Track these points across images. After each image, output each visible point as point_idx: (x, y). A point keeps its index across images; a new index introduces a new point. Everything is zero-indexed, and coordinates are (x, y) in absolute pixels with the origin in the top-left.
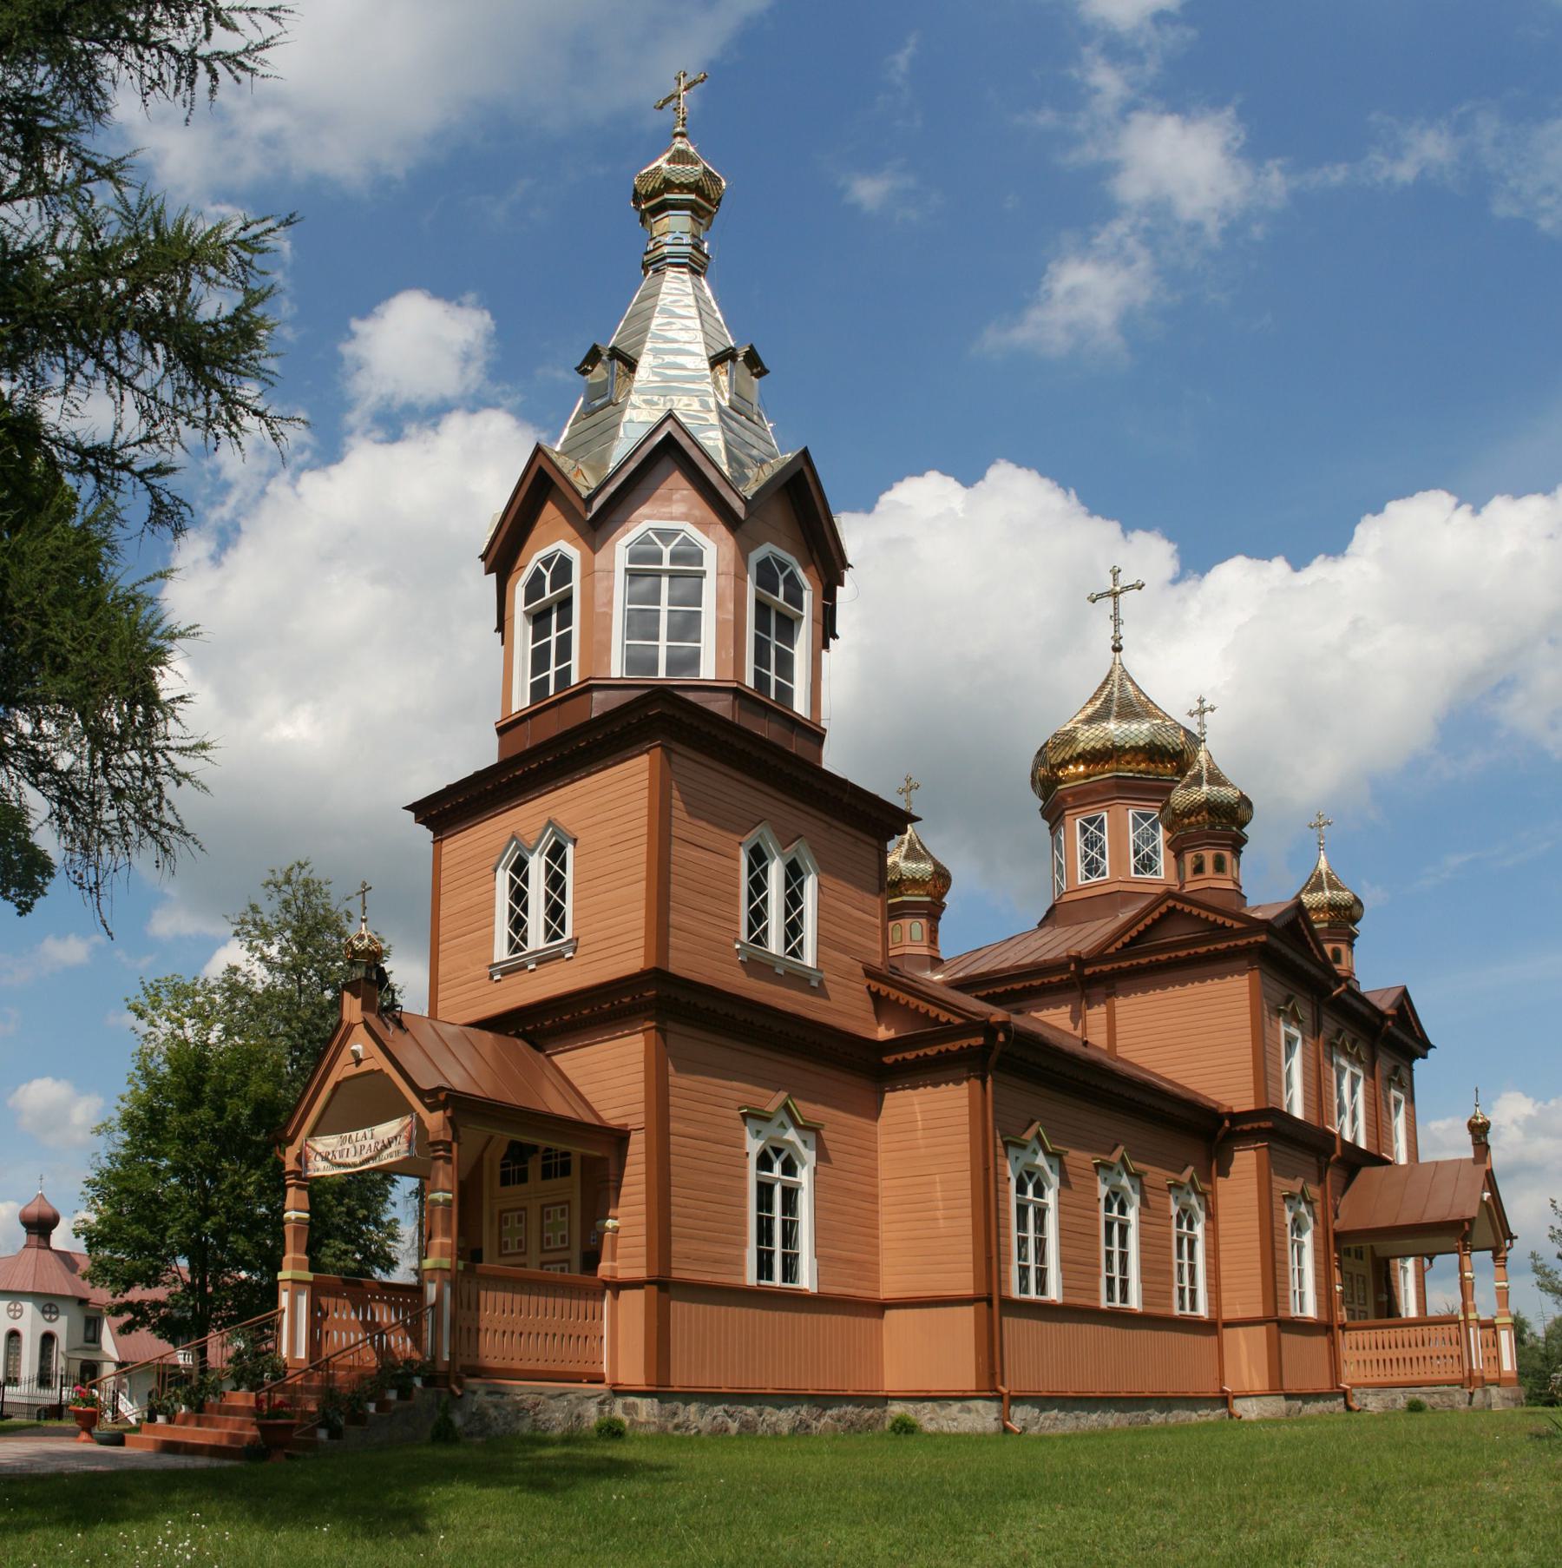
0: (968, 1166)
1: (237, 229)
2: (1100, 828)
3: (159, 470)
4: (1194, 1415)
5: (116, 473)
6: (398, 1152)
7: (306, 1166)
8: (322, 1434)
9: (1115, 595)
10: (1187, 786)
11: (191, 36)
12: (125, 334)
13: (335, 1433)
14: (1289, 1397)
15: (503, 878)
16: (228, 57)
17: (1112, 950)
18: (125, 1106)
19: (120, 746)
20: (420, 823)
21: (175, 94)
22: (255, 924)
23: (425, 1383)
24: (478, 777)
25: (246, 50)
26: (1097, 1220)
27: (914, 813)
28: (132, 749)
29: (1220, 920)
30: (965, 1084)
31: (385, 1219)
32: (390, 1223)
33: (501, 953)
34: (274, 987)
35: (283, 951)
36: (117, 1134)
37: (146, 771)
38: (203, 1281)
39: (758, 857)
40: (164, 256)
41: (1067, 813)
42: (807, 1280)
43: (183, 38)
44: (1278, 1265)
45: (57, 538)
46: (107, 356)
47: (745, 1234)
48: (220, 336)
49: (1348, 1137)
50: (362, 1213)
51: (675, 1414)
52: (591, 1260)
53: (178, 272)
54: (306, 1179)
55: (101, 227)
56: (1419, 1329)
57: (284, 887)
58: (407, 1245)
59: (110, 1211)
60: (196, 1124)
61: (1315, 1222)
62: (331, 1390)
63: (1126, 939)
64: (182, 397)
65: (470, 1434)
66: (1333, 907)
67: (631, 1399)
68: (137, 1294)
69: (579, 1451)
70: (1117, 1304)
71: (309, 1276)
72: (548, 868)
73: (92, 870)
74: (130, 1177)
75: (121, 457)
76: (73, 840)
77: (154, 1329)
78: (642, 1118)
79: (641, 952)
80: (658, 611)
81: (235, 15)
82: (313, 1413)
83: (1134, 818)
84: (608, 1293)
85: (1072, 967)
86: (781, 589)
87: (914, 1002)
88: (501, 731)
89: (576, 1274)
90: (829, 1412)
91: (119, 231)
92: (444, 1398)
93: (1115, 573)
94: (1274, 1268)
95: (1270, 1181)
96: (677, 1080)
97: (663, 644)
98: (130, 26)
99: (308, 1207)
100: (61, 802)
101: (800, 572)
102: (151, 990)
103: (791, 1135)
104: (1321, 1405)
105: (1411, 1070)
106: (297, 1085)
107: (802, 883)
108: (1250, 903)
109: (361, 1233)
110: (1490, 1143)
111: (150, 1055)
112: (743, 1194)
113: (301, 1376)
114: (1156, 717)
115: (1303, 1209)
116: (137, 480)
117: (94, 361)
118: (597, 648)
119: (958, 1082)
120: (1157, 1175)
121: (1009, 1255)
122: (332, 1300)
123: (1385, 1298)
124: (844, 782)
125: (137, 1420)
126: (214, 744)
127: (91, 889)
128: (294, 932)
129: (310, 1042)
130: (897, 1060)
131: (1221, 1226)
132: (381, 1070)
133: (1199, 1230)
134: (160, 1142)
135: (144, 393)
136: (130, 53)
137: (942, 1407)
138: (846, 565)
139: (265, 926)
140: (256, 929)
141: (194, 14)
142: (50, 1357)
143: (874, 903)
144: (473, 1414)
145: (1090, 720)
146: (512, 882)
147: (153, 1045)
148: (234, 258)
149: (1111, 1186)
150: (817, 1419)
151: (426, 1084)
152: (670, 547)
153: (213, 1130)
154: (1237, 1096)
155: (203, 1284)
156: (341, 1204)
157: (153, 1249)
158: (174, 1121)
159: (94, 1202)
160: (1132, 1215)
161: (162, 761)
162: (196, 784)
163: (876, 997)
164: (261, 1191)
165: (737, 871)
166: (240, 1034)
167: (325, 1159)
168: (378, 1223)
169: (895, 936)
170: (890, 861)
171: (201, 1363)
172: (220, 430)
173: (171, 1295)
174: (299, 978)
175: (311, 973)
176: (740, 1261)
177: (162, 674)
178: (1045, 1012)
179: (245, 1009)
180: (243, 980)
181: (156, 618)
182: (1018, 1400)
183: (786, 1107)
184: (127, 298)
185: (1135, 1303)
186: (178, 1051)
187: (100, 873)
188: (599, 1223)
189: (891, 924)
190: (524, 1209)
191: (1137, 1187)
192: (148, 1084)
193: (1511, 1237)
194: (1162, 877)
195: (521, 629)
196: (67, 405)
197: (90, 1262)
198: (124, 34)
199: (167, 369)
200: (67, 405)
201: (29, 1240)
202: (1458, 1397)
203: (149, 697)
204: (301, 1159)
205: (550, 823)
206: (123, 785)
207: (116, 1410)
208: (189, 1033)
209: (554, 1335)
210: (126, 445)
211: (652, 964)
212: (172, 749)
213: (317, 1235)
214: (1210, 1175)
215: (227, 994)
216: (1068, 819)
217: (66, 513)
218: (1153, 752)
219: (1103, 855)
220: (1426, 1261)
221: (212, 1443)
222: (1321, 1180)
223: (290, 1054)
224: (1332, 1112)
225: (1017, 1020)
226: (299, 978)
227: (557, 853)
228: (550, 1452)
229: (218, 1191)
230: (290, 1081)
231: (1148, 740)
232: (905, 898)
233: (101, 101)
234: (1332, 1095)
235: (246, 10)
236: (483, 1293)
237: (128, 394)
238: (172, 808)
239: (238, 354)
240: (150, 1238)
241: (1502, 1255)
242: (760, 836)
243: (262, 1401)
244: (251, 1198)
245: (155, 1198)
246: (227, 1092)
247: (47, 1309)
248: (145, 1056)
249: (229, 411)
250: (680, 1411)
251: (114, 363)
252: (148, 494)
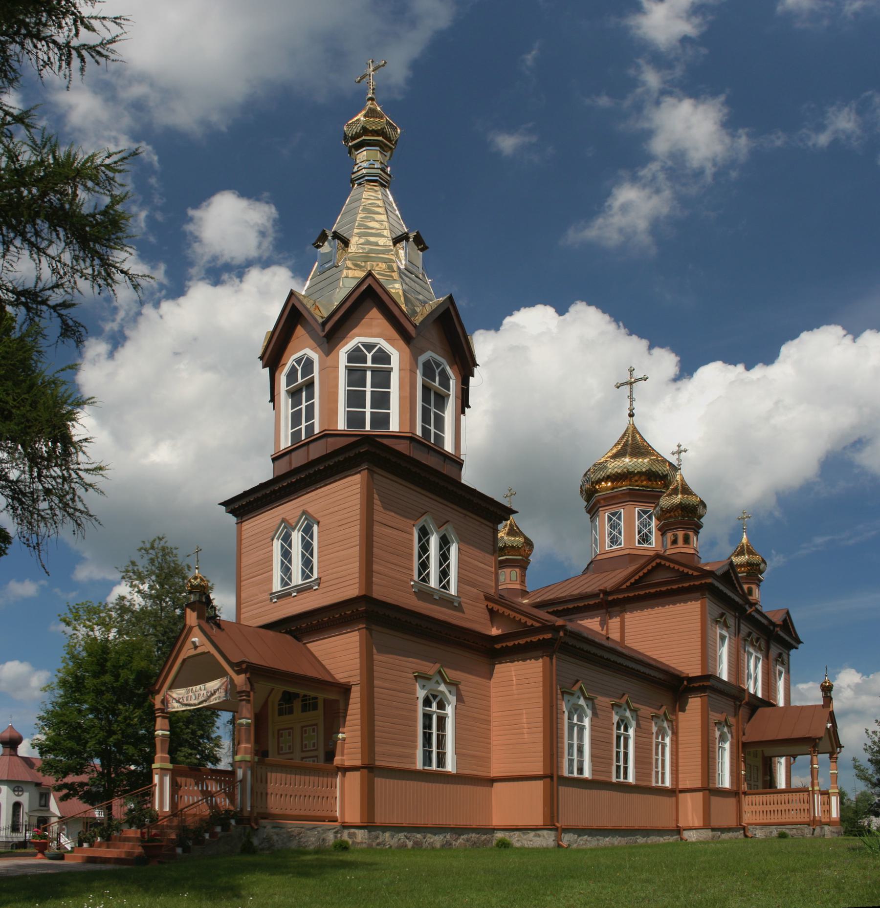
0: (541, 705)
1: (103, 157)
2: (619, 518)
3: (65, 305)
4: (661, 839)
5: (39, 307)
6: (220, 697)
7: (167, 706)
8: (179, 850)
9: (631, 383)
10: (670, 495)
11: (66, 34)
12: (39, 221)
13: (186, 850)
14: (713, 829)
15: (277, 545)
16: (91, 48)
17: (624, 586)
18: (61, 675)
19: (48, 464)
20: (229, 512)
21: (59, 71)
22: (134, 572)
23: (237, 823)
25: (102, 43)
26: (612, 734)
27: (514, 508)
28: (55, 466)
29: (686, 570)
30: (541, 660)
31: (213, 736)
32: (216, 738)
33: (277, 586)
34: (146, 608)
35: (151, 587)
36: (56, 691)
37: (64, 479)
38: (109, 771)
39: (424, 533)
40: (60, 174)
41: (600, 509)
42: (450, 766)
43: (61, 35)
44: (710, 760)
45: (5, 346)
46: (29, 235)
47: (416, 741)
48: (98, 223)
49: (752, 691)
50: (200, 733)
51: (377, 837)
52: (330, 756)
53: (69, 184)
54: (167, 713)
55: (19, 155)
56: (787, 794)
57: (151, 551)
58: (226, 750)
59: (53, 734)
60: (104, 684)
61: (732, 736)
62: (184, 826)
63: (632, 580)
64: (77, 261)
65: (262, 849)
66: (749, 564)
67: (352, 830)
68: (71, 779)
69: (324, 857)
70: (622, 780)
71: (170, 766)
72: (303, 538)
73: (34, 536)
74: (65, 714)
75: (41, 297)
76: (22, 520)
77: (81, 798)
78: (358, 678)
79: (357, 585)
80: (365, 391)
81: (93, 21)
82: (174, 839)
83: (638, 512)
84: (340, 773)
85: (601, 596)
86: (437, 379)
87: (512, 614)
88: (274, 460)
89: (321, 763)
90: (462, 837)
91: (30, 157)
92: (248, 831)
93: (631, 371)
94: (708, 761)
95: (708, 714)
96: (377, 657)
97: (368, 410)
98: (27, 25)
99: (168, 728)
100: (13, 498)
101: (448, 368)
102: (74, 611)
103: (442, 688)
104: (731, 834)
105: (789, 655)
106: (161, 662)
107: (449, 548)
108: (703, 561)
109: (200, 744)
110: (832, 696)
111: (74, 647)
112: (415, 720)
113: (166, 820)
114: (653, 455)
115: (726, 730)
116: (52, 311)
117: (21, 238)
118: (330, 412)
119: (536, 658)
120: (646, 711)
121: (563, 753)
122: (183, 779)
123: (768, 778)
124: (475, 490)
125: (72, 848)
126: (107, 467)
127: (34, 547)
128: (157, 576)
129: (168, 638)
130: (502, 646)
131: (680, 739)
132: (209, 652)
133: (668, 740)
134: (82, 694)
135: (53, 258)
136: (29, 44)
137: (524, 834)
138: (476, 365)
139: (140, 573)
140: (135, 575)
141: (67, 20)
142: (19, 815)
143: (491, 559)
144: (264, 839)
145: (615, 456)
146: (282, 546)
147: (75, 641)
148: (103, 175)
149: (621, 716)
150: (456, 840)
151: (235, 660)
152: (372, 353)
153: (113, 687)
154: (692, 668)
155: (109, 773)
156: (188, 728)
157: (79, 754)
158: (90, 683)
159: (44, 729)
160: (631, 732)
161: (74, 475)
162: (97, 490)
163: (491, 611)
164: (142, 721)
165: (412, 540)
166: (127, 634)
167: (178, 701)
168: (209, 739)
169: (502, 578)
170: (499, 535)
171: (109, 815)
172: (101, 282)
173: (90, 779)
174: (161, 602)
175: (168, 599)
176: (413, 757)
177: (73, 426)
178: (586, 621)
179: (129, 621)
180: (128, 604)
181: (68, 393)
182: (567, 830)
183: (440, 672)
184: (39, 199)
185: (631, 779)
186: (91, 644)
187: (40, 537)
188: (334, 735)
189: (500, 571)
190: (292, 728)
191: (635, 717)
192: (74, 663)
193: (841, 747)
194: (654, 546)
195: (285, 400)
196: (6, 264)
197: (42, 762)
198: (23, 31)
199: (67, 244)
200: (6, 264)
201: (4, 751)
202: (806, 831)
203: (66, 440)
204: (164, 702)
205: (304, 513)
206: (51, 487)
207: (59, 842)
208: (97, 634)
209: (310, 796)
210: (44, 289)
211: (363, 593)
212: (81, 470)
213: (174, 745)
214: (675, 711)
215: (119, 612)
216: (601, 513)
217: (9, 330)
218: (651, 475)
219: (620, 534)
220: (792, 759)
221: (116, 856)
222: (736, 714)
223: (157, 645)
224: (744, 678)
225: (570, 626)
226: (161, 602)
227: (308, 530)
228: (309, 857)
229: (116, 721)
230: (157, 661)
231: (648, 468)
232: (508, 557)
233: (12, 73)
234: (744, 668)
235: (99, 18)
236: (269, 774)
237: (43, 259)
238: (81, 501)
239: (109, 235)
240: (78, 748)
241: (835, 756)
242: (425, 521)
243: (144, 833)
244: (136, 724)
245: (79, 726)
246: (120, 666)
247: (16, 789)
248: (71, 648)
249: (106, 270)
250: (380, 836)
251: (33, 239)
252: (59, 319)
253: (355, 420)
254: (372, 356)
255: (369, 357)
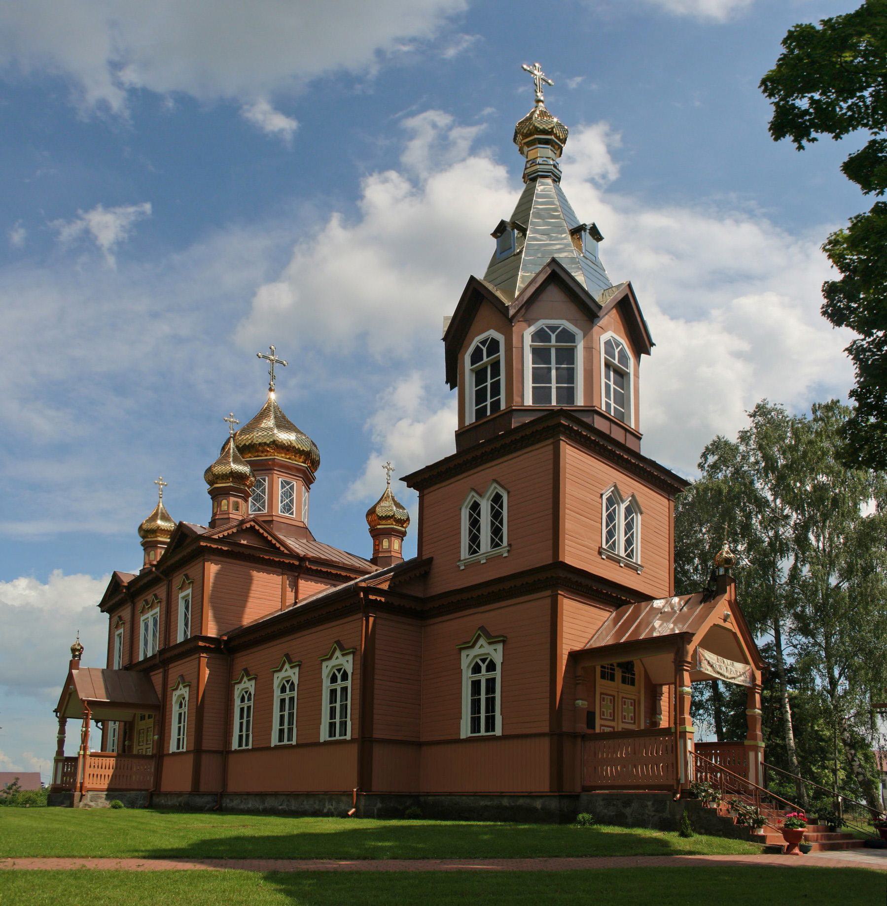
24: (447, 460)
253: (541, 394)
254: (556, 336)
255: (553, 337)
